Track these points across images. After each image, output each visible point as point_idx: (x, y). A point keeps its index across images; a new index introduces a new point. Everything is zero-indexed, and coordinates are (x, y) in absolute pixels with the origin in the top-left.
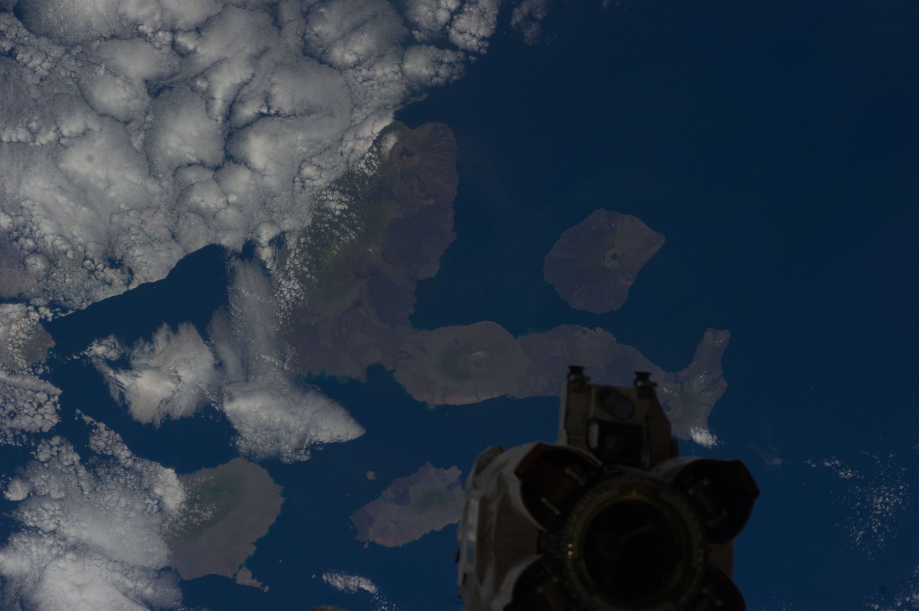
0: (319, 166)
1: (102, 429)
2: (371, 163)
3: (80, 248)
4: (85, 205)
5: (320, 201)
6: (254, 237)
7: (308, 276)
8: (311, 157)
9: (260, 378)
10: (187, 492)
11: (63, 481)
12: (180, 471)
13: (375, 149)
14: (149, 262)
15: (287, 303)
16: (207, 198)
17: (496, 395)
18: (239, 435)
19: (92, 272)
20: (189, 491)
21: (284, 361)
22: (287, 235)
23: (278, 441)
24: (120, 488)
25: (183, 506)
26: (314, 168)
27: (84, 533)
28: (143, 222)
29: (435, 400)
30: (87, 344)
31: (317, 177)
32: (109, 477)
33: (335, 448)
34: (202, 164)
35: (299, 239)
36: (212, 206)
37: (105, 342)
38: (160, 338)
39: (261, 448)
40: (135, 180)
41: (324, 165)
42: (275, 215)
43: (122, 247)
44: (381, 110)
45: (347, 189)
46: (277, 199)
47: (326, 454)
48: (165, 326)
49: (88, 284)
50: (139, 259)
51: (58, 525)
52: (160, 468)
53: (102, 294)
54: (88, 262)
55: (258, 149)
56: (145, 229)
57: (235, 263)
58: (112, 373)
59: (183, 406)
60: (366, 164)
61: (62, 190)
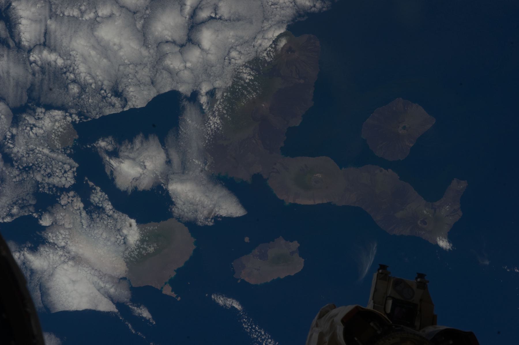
0: (240, 52)
1: (98, 191)
2: (270, 54)
3: (100, 83)
5: (238, 72)
6: (198, 89)
7: (226, 116)
8: (236, 46)
9: (191, 173)
10: (141, 234)
13: (273, 46)
14: (137, 96)
15: (212, 130)
16: (174, 62)
17: (325, 201)
18: (175, 205)
19: (104, 97)
20: (142, 234)
21: (206, 165)
22: (217, 90)
23: (197, 212)
24: (104, 227)
25: (138, 242)
26: (237, 53)
27: (80, 250)
28: (137, 72)
29: (290, 200)
30: (96, 139)
31: (238, 58)
32: (98, 219)
33: (229, 220)
34: (174, 42)
35: (223, 95)
36: (177, 68)
37: (106, 140)
38: (137, 142)
39: (186, 214)
40: (135, 47)
41: (243, 52)
42: (212, 77)
43: (123, 85)
45: (254, 68)
46: (214, 69)
47: (223, 223)
48: (141, 135)
49: (101, 105)
50: (131, 93)
51: (67, 243)
52: (128, 218)
53: (108, 111)
54: (103, 91)
55: (207, 37)
56: (138, 76)
57: (185, 103)
59: (145, 184)
60: (267, 54)
61: (94, 48)
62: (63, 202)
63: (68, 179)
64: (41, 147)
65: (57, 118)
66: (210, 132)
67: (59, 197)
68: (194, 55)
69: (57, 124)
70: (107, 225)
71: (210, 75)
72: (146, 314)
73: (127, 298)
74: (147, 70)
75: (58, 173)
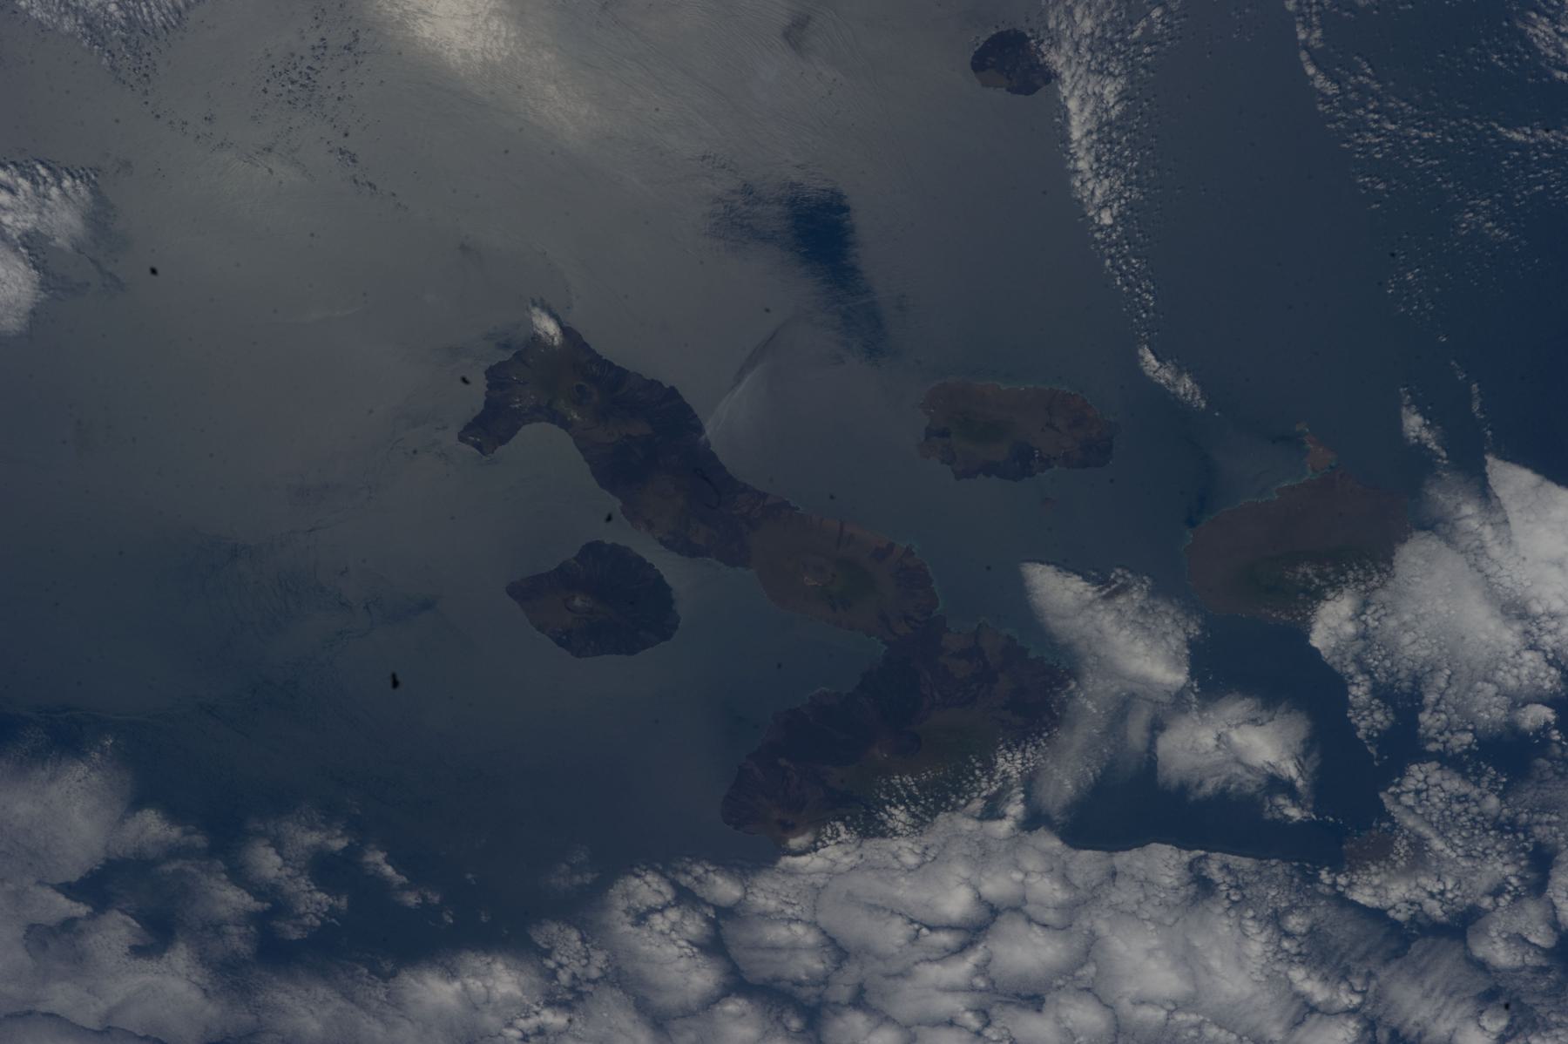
3: (1232, 913)
4: (1195, 947)
9: (1115, 689)
10: (1314, 610)
11: (1464, 698)
12: (1303, 635)
15: (1024, 751)
16: (1047, 890)
18: (1189, 640)
19: (1238, 887)
23: (1142, 608)
24: (1397, 656)
25: (1330, 595)
28: (1139, 903)
31: (906, 850)
32: (1402, 675)
34: (1030, 920)
37: (1278, 816)
38: (1209, 788)
41: (889, 856)
43: (1182, 893)
44: (791, 872)
46: (966, 851)
53: (1247, 863)
54: (1234, 898)
55: (956, 903)
56: (1141, 895)
58: (1300, 783)
59: (1236, 708)
62: (1467, 738)
63: (1421, 777)
64: (1444, 855)
65: (1368, 891)
66: (1030, 749)
67: (1466, 752)
68: (997, 886)
69: (1376, 881)
70: (1385, 657)
71: (978, 843)
72: (1413, 423)
73: (1439, 476)
74: (1114, 899)
75: (1437, 798)
